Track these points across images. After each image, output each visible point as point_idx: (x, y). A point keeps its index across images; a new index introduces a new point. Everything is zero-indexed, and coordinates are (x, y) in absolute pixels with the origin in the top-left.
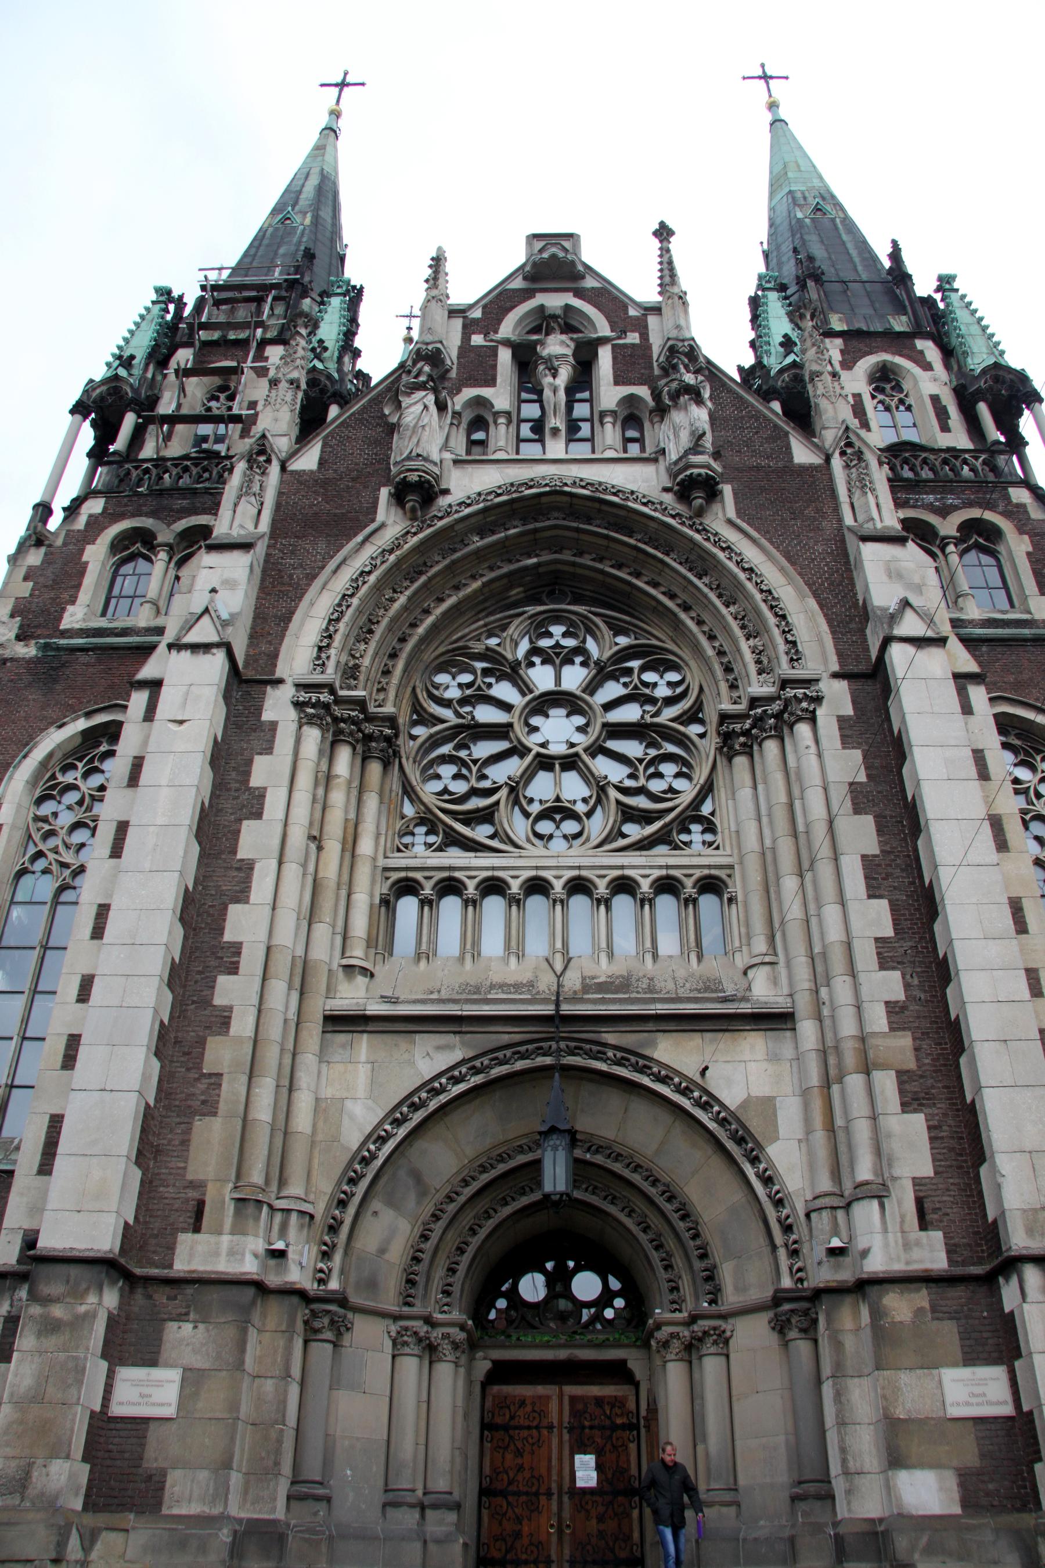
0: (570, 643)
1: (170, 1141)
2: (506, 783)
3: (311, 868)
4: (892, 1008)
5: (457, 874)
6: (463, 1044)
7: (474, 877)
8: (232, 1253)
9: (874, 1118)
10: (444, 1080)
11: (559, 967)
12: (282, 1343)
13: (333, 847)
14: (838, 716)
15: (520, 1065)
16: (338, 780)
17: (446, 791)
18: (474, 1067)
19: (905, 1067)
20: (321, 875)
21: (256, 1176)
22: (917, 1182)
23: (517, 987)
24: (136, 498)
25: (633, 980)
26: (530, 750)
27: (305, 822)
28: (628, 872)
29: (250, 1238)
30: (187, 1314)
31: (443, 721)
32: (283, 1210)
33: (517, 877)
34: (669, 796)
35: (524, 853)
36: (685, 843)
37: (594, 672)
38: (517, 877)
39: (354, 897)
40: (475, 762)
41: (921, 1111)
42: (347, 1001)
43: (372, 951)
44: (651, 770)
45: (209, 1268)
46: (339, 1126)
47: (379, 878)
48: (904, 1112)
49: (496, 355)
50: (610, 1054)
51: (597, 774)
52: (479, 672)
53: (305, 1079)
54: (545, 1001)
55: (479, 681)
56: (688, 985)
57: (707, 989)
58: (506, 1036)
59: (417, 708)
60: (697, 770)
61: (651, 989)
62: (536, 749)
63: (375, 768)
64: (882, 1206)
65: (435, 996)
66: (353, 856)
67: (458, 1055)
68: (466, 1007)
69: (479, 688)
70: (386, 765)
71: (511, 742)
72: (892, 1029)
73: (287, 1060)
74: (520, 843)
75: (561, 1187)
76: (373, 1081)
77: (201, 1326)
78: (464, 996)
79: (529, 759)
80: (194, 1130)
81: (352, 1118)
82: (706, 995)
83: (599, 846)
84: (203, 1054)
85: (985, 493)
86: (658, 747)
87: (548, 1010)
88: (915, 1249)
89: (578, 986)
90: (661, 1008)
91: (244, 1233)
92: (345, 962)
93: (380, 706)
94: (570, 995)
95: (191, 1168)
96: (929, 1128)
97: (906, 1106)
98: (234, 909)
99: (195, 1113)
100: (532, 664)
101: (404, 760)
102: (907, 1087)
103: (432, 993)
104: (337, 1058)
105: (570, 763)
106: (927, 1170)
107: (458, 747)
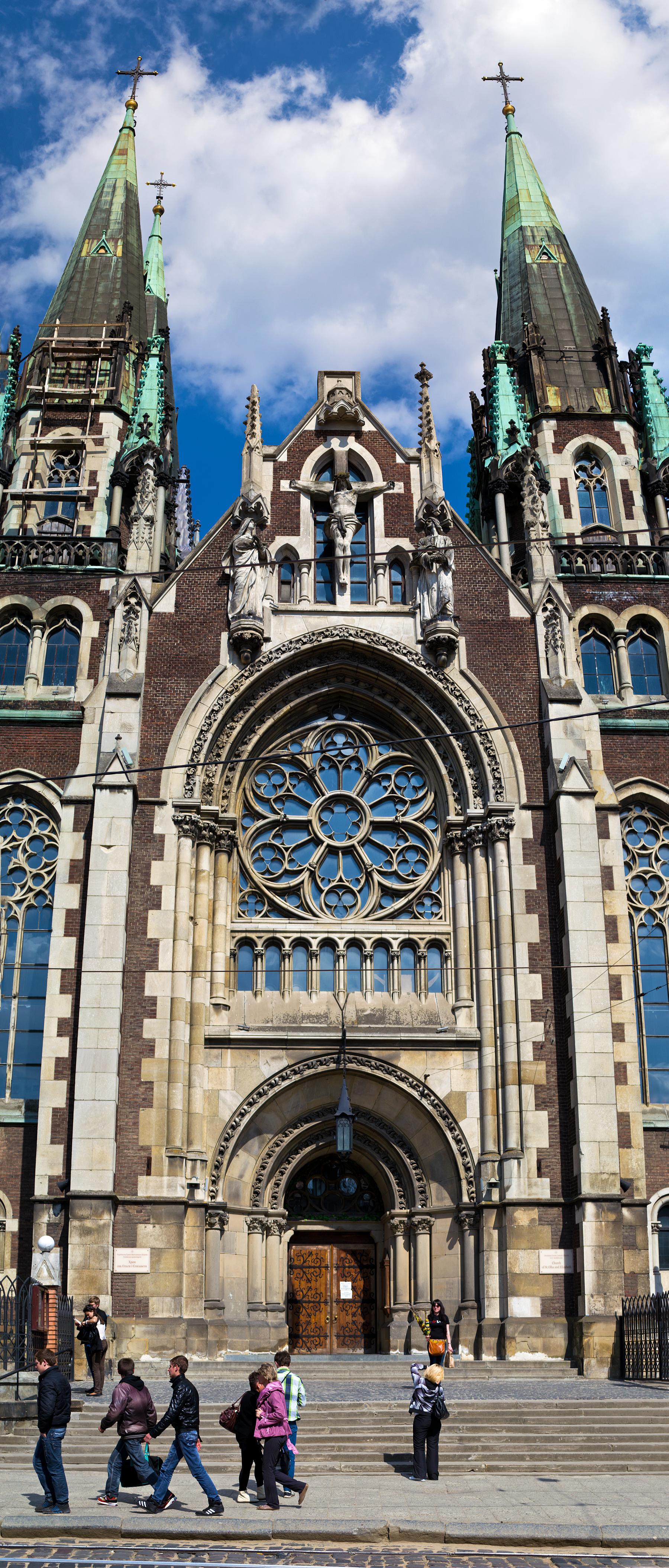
0: (349, 752)
1: (127, 1123)
2: (308, 869)
3: (191, 941)
4: (538, 1047)
5: (278, 935)
6: (288, 1056)
7: (289, 938)
8: (170, 1186)
9: (521, 1112)
10: (277, 1079)
11: (342, 1001)
12: (198, 1232)
13: (203, 923)
14: (523, 839)
15: (321, 1069)
16: (204, 874)
17: (268, 872)
18: (294, 1070)
19: (540, 1083)
20: (197, 944)
21: (178, 1143)
22: (539, 1151)
23: (318, 1017)
24: (12, 576)
25: (387, 1013)
26: (322, 842)
27: (186, 910)
28: (384, 936)
29: (179, 1178)
30: (149, 1220)
31: (265, 818)
32: (192, 1160)
33: (316, 938)
34: (411, 878)
35: (320, 920)
36: (420, 914)
37: (365, 779)
38: (316, 938)
39: (216, 954)
40: (287, 849)
41: (546, 1110)
42: (217, 1029)
43: (228, 989)
44: (401, 858)
45: (158, 1195)
46: (217, 1107)
47: (229, 938)
48: (536, 1110)
49: (299, 503)
50: (373, 1063)
51: (366, 862)
52: (287, 776)
53: (196, 1080)
54: (335, 1029)
55: (288, 784)
56: (419, 1018)
57: (431, 1022)
58: (313, 1051)
59: (247, 806)
60: (431, 858)
61: (397, 1021)
62: (327, 841)
63: (223, 858)
64: (519, 1163)
65: (270, 1025)
66: (213, 925)
67: (285, 1063)
68: (290, 1034)
69: (288, 790)
70: (230, 855)
71: (310, 834)
72: (535, 1059)
73: (187, 1070)
74: (318, 913)
75: (347, 1148)
76: (236, 1080)
77: (157, 1226)
78: (287, 1025)
79: (323, 848)
80: (141, 1116)
81: (225, 1102)
82: (430, 1026)
83: (366, 916)
84: (140, 1070)
85: (652, 589)
86: (407, 840)
87: (338, 1036)
88: (534, 1188)
89: (354, 1019)
90: (404, 1036)
91: (175, 1175)
92: (214, 1001)
93: (225, 811)
94: (350, 1024)
95: (141, 1139)
96: (550, 1120)
97: (538, 1107)
98: (149, 976)
99: (139, 1106)
100: (322, 769)
101: (240, 848)
102: (540, 1095)
103: (268, 1022)
104: (213, 1064)
105: (349, 851)
106: (545, 1144)
107: (274, 837)
